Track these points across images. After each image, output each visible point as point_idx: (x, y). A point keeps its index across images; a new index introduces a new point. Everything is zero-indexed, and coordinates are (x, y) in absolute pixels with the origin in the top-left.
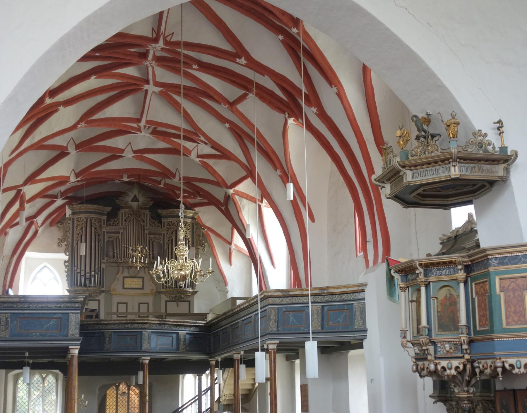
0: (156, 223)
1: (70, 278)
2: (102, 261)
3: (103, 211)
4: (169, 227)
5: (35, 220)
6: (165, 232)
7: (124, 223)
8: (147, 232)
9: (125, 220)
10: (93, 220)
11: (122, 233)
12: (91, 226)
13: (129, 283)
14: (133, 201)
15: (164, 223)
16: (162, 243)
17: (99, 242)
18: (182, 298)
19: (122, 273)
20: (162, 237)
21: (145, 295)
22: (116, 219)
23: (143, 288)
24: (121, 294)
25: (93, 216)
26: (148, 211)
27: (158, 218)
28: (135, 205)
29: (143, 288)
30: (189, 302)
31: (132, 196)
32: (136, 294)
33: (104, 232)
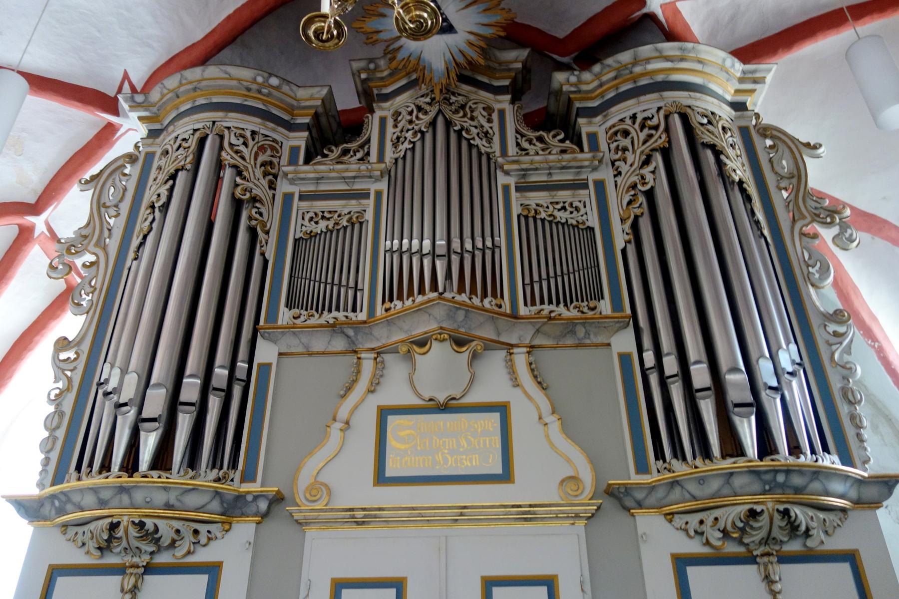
0: (555, 142)
1: (61, 434)
2: (262, 323)
3: (290, 110)
4: (626, 142)
5: (38, 222)
6: (606, 174)
8: (511, 181)
10: (230, 138)
12: (219, 166)
13: (417, 444)
15: (593, 137)
16: (593, 221)
17: (253, 232)
18: (793, 527)
19: (371, 391)
20: (589, 195)
21: (527, 514)
22: (353, 145)
23: (506, 476)
24: (360, 518)
25: (234, 120)
27: (556, 120)
29: (506, 476)
30: (851, 558)
32: (462, 515)
33: (288, 197)
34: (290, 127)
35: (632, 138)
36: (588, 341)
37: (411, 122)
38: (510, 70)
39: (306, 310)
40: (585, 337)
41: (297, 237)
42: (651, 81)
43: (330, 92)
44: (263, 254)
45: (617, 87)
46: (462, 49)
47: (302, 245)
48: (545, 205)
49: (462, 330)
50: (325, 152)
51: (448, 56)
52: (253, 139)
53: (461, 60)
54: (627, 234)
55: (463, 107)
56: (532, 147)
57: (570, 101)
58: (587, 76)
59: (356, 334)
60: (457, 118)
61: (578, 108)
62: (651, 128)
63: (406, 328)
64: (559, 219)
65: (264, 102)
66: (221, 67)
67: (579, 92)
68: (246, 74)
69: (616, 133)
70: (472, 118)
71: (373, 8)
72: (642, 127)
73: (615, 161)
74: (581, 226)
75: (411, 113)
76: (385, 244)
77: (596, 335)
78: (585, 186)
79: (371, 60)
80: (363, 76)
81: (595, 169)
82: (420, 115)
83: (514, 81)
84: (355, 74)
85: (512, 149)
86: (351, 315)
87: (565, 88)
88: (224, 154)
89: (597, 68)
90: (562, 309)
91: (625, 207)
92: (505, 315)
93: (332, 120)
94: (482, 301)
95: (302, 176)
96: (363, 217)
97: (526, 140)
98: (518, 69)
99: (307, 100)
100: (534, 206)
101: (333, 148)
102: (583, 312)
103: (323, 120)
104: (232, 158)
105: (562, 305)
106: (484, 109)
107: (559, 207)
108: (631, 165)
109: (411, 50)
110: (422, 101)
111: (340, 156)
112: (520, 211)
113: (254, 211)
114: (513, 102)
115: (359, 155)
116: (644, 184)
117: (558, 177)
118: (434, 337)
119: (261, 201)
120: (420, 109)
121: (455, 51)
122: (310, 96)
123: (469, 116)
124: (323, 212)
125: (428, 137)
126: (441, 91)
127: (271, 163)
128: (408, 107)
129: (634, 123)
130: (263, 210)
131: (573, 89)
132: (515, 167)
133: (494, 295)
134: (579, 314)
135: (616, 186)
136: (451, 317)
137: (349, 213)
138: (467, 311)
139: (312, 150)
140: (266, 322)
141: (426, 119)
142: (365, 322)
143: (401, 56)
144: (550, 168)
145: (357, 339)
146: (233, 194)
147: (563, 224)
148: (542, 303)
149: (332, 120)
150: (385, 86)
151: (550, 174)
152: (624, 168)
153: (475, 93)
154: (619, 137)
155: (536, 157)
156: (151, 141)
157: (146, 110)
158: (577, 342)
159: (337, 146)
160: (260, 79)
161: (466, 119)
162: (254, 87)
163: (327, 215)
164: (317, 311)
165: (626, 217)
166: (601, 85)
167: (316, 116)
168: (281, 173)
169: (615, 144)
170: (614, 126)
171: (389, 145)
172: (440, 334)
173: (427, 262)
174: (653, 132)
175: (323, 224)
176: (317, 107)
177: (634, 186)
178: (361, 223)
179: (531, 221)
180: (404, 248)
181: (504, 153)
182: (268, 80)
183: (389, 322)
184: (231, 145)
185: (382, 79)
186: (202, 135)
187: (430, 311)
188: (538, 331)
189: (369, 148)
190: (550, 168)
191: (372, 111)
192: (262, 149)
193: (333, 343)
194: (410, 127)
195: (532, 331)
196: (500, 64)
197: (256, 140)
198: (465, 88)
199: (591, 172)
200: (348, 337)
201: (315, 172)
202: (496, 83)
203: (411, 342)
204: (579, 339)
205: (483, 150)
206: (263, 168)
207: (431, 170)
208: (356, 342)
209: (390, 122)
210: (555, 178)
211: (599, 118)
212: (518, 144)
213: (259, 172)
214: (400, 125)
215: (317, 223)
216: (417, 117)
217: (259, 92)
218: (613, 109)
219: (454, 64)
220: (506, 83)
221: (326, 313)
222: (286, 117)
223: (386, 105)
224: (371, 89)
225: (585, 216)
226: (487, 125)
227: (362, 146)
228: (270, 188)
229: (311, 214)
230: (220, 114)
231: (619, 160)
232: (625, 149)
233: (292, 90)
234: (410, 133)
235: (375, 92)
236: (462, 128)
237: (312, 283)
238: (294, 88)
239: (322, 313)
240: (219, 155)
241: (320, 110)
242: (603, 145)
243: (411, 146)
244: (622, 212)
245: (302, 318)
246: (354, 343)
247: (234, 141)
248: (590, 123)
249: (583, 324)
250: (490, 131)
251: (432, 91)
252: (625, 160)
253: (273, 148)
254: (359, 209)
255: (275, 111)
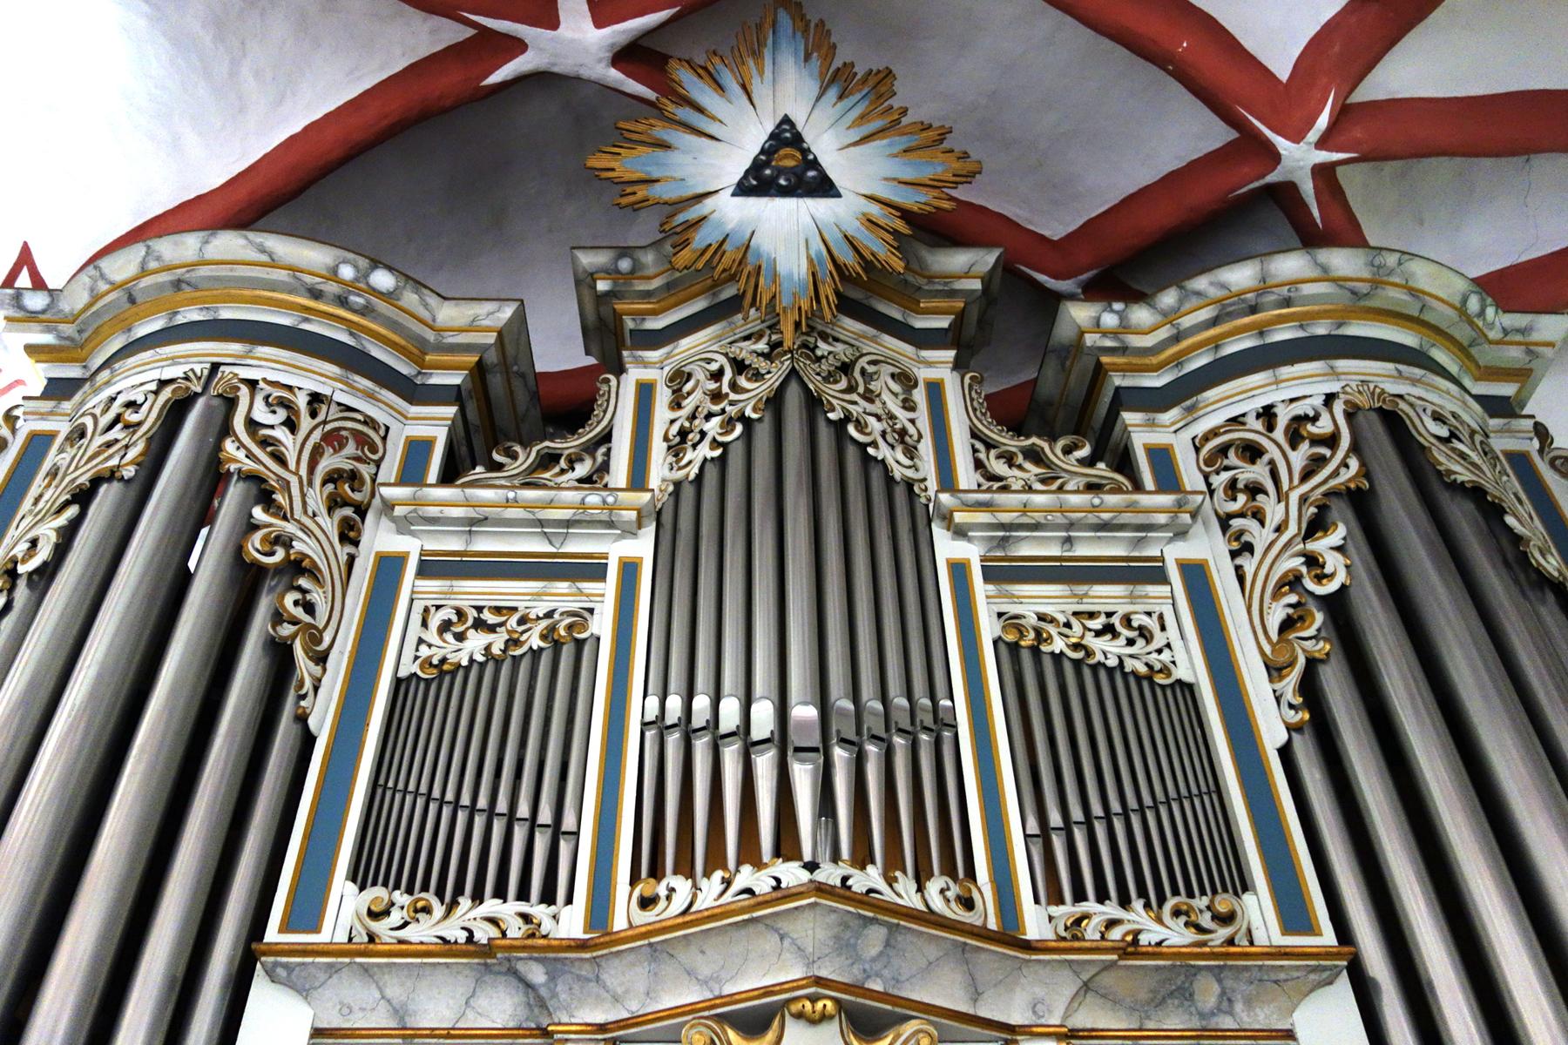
2: (272, 934)
3: (418, 351)
4: (1257, 472)
6: (1207, 546)
7: (659, 471)
8: (972, 552)
9: (679, 443)
11: (629, 569)
14: (759, 181)
15: (1162, 458)
16: (1190, 665)
17: (280, 658)
20: (1169, 601)
22: (569, 445)
26: (950, 354)
27: (1064, 414)
28: (785, 233)
31: (745, 137)
33: (389, 567)
34: (414, 392)
35: (1272, 462)
36: (1227, 1022)
37: (717, 396)
38: (953, 294)
39: (410, 891)
40: (1219, 1010)
41: (403, 673)
42: (1300, 334)
43: (520, 318)
44: (302, 719)
45: (1216, 343)
46: (850, 233)
47: (416, 695)
48: (1062, 619)
49: (877, 986)
50: (497, 457)
51: (817, 245)
52: (313, 414)
53: (847, 257)
54: (1291, 706)
55: (846, 368)
56: (1016, 472)
57: (1099, 372)
58: (1141, 315)
59: (552, 977)
60: (832, 392)
61: (1118, 389)
62: (1316, 441)
63: (705, 971)
64: (1099, 657)
65: (351, 327)
66: (251, 235)
67: (1123, 350)
68: (312, 256)
69: (1223, 450)
70: (869, 396)
71: (640, 128)
72: (1294, 438)
73: (1231, 516)
74: (1160, 679)
75: (717, 376)
76: (641, 706)
77: (1249, 1002)
78: (1159, 576)
79: (624, 252)
80: (602, 286)
81: (1181, 534)
82: (743, 382)
83: (961, 317)
84: (583, 282)
85: (966, 476)
86: (540, 911)
87: (1090, 339)
88: (229, 446)
89: (1168, 298)
90: (1138, 915)
91: (1274, 636)
92: (982, 933)
93: (517, 384)
94: (920, 889)
95: (433, 511)
96: (584, 628)
97: (998, 457)
98: (973, 291)
99: (461, 330)
100: (1033, 620)
101: (518, 448)
102: (1200, 929)
103: (496, 382)
104: (250, 455)
105: (1138, 904)
106: (893, 376)
107: (1097, 624)
108: (1279, 529)
109: (729, 227)
110: (745, 350)
111: (532, 470)
112: (998, 632)
113: (290, 599)
114: (959, 365)
115: (582, 470)
116: (1320, 578)
117: (1088, 548)
118: (795, 1007)
119: (313, 573)
120: (740, 366)
121: (834, 238)
122: (468, 319)
123: (861, 389)
124: (479, 609)
125: (763, 435)
126: (797, 325)
127: (354, 477)
128: (709, 361)
129: (1271, 427)
130: (317, 596)
131: (1109, 343)
132: (983, 517)
133: (949, 870)
134: (1190, 936)
135: (1241, 578)
136: (844, 945)
137: (549, 615)
138: (890, 926)
139: (464, 450)
140: (285, 927)
141: (755, 391)
142: (582, 945)
143: (701, 238)
144: (1071, 526)
145: (554, 995)
146: (239, 550)
147: (1110, 671)
148: (1080, 896)
149: (517, 384)
150: (654, 313)
151: (1068, 541)
152: (1260, 536)
153: (873, 339)
154: (1232, 459)
155: (1027, 494)
156: (48, 405)
157: (48, 330)
158: (1196, 1023)
159: (526, 445)
160: (347, 272)
161: (854, 397)
162: (332, 288)
163: (491, 618)
164: (440, 894)
165: (1282, 659)
166: (1177, 338)
167: (480, 371)
168: (377, 501)
169: (1225, 476)
170: (1214, 433)
171: (658, 448)
172: (813, 999)
173: (764, 764)
174: (1326, 452)
175: (476, 643)
176: (483, 348)
177: (1292, 582)
178: (580, 644)
179: (1026, 659)
180: (698, 720)
181: (947, 481)
182: (366, 276)
183: (656, 944)
184: (252, 425)
185: (647, 295)
186: (180, 395)
187: (784, 926)
188: (1086, 987)
189: (608, 454)
190: (1071, 526)
191: (620, 370)
192: (333, 439)
193: (482, 1002)
194: (716, 408)
195: (1067, 987)
196: (931, 278)
197: (321, 418)
198: (850, 325)
199: (1171, 540)
200: (528, 986)
201: (468, 504)
202: (920, 323)
203: (720, 1018)
204: (1202, 1015)
205: (898, 473)
206: (330, 487)
207: (771, 513)
208: (551, 1004)
209: (663, 396)
210: (1081, 550)
211: (1174, 413)
212: (979, 465)
213: (317, 498)
214: (689, 404)
215: (460, 637)
216: (734, 386)
217: (342, 301)
218: (1212, 394)
219: (830, 266)
220: (943, 322)
221: (465, 902)
222: (404, 368)
223: (653, 355)
224: (618, 317)
225: (1166, 652)
226: (902, 416)
227: (590, 448)
228: (344, 538)
229: (448, 614)
230: (236, 347)
231: (1241, 515)
232: (1254, 490)
233: (426, 306)
234: (716, 421)
235: (630, 324)
236: (847, 418)
237: (433, 807)
238: (433, 300)
239: (454, 903)
240: (218, 447)
241: (492, 357)
242: (1191, 477)
243: (718, 453)
244: (1267, 649)
245: (396, 917)
246: (542, 1004)
247: (261, 414)
248: (1152, 424)
249: (1217, 973)
250: (911, 430)
251: (773, 327)
252: (1259, 516)
253: (362, 440)
254: (574, 606)
255: (378, 352)
